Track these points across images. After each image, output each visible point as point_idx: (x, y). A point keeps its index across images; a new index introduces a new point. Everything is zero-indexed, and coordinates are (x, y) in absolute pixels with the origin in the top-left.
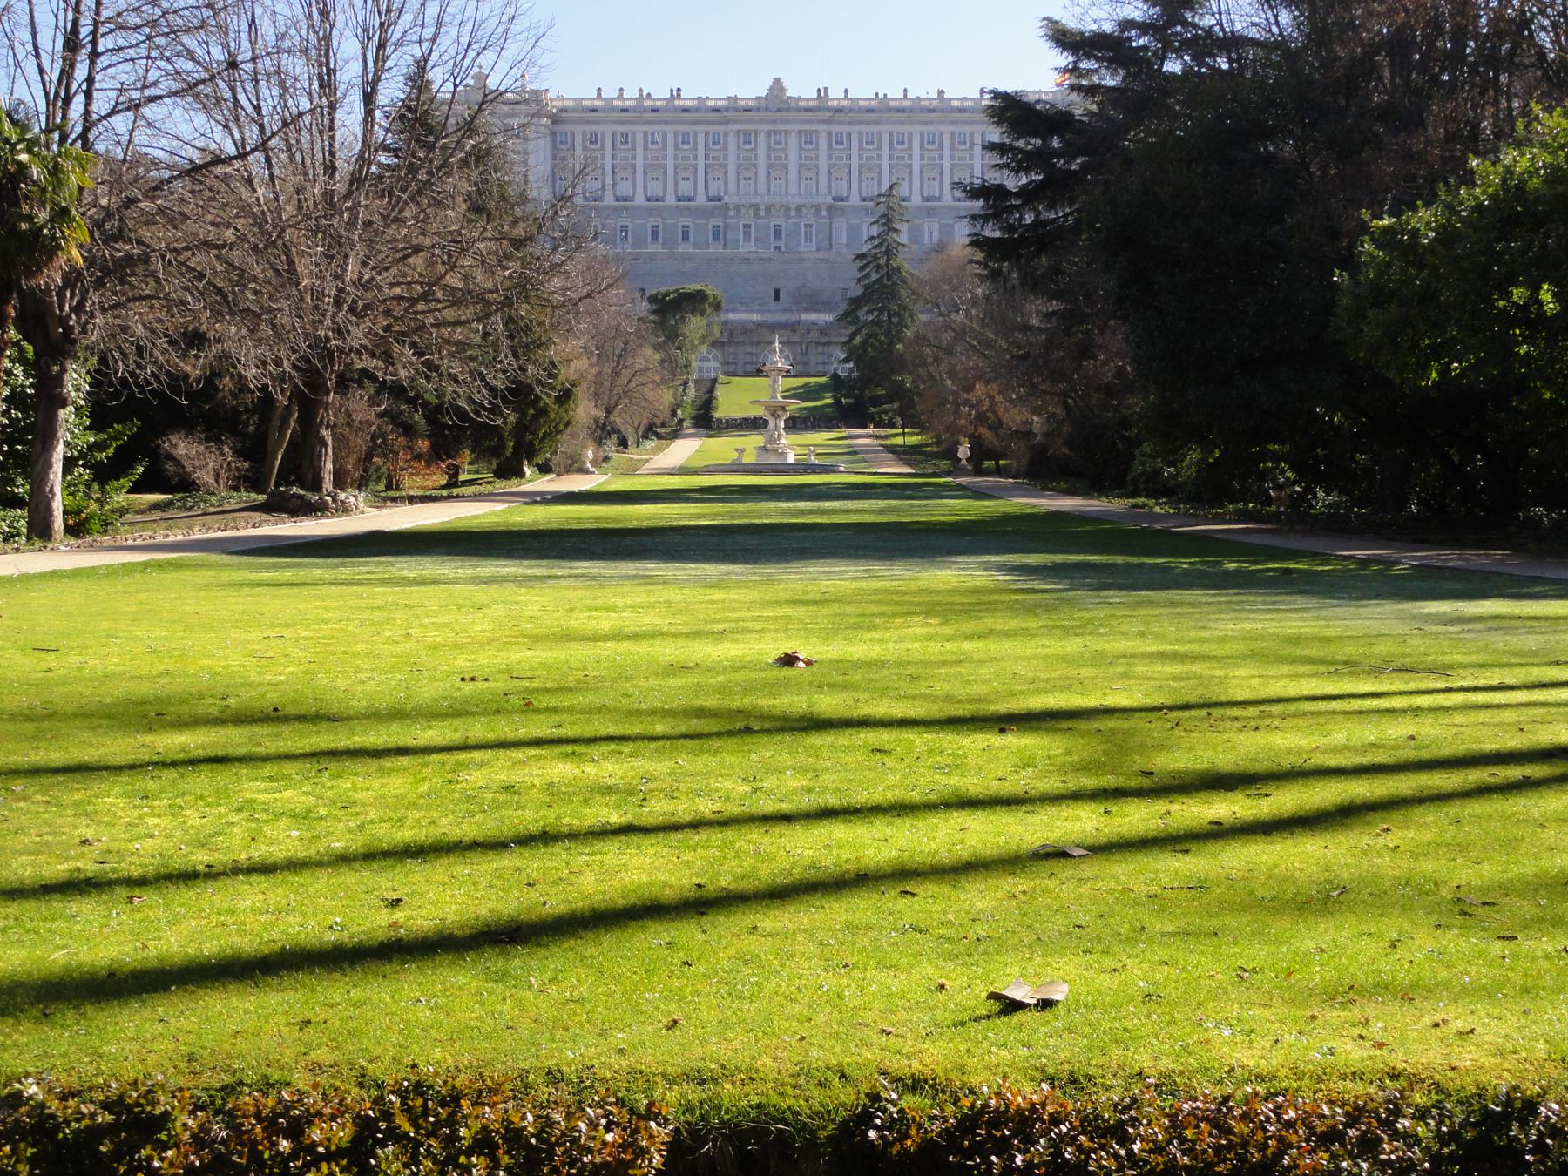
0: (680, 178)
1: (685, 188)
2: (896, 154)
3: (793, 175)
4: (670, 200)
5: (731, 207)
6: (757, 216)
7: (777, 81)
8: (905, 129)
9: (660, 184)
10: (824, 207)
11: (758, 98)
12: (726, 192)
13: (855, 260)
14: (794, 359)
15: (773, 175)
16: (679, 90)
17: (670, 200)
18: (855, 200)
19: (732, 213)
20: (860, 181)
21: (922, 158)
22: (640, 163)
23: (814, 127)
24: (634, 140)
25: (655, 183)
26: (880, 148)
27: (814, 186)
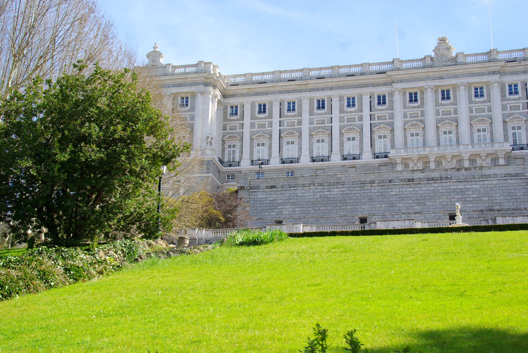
0: (345, 139)
1: (350, 148)
3: (464, 127)
7: (442, 40)
9: (326, 145)
10: (501, 155)
12: (393, 147)
15: (442, 129)
17: (336, 159)
22: (305, 128)
24: (300, 106)
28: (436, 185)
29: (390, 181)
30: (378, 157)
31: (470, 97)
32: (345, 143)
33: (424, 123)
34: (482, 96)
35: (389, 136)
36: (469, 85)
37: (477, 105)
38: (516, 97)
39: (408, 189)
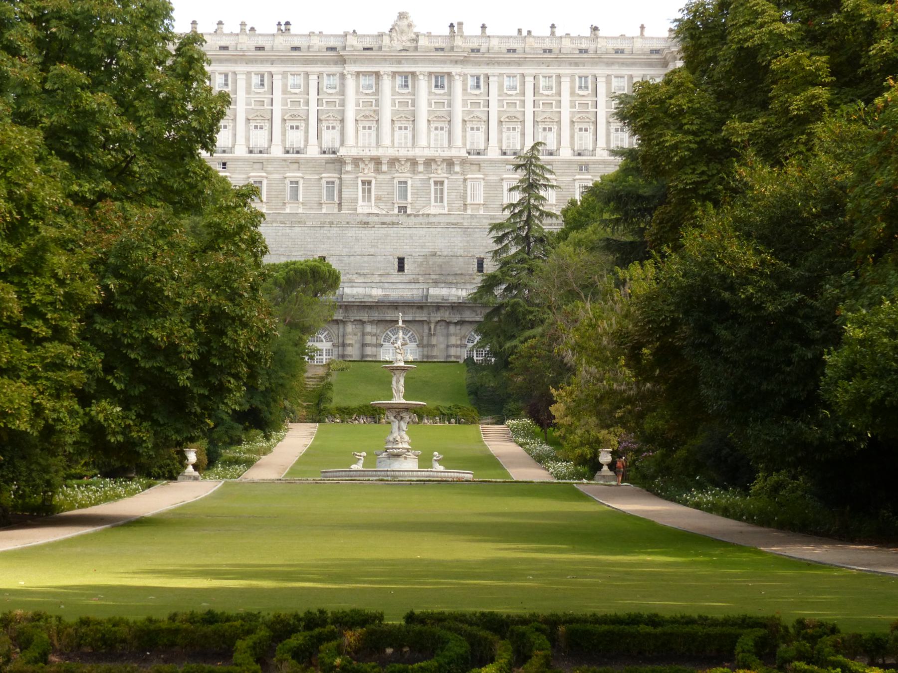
1: (295, 138)
2: (541, 100)
4: (277, 151)
5: (348, 161)
6: (378, 171)
7: (402, 16)
8: (553, 71)
11: (381, 35)
12: (342, 143)
13: (491, 231)
14: (421, 340)
16: (287, 23)
18: (493, 153)
19: (349, 168)
20: (500, 132)
21: (573, 106)
23: (445, 69)
25: (259, 131)
26: (523, 93)
27: (446, 135)
28: (387, 229)
29: (348, 223)
30: (324, 152)
31: (429, 87)
32: (287, 131)
33: (377, 115)
34: (443, 87)
35: (338, 128)
36: (430, 74)
37: (437, 97)
38: (477, 92)
39: (363, 232)
